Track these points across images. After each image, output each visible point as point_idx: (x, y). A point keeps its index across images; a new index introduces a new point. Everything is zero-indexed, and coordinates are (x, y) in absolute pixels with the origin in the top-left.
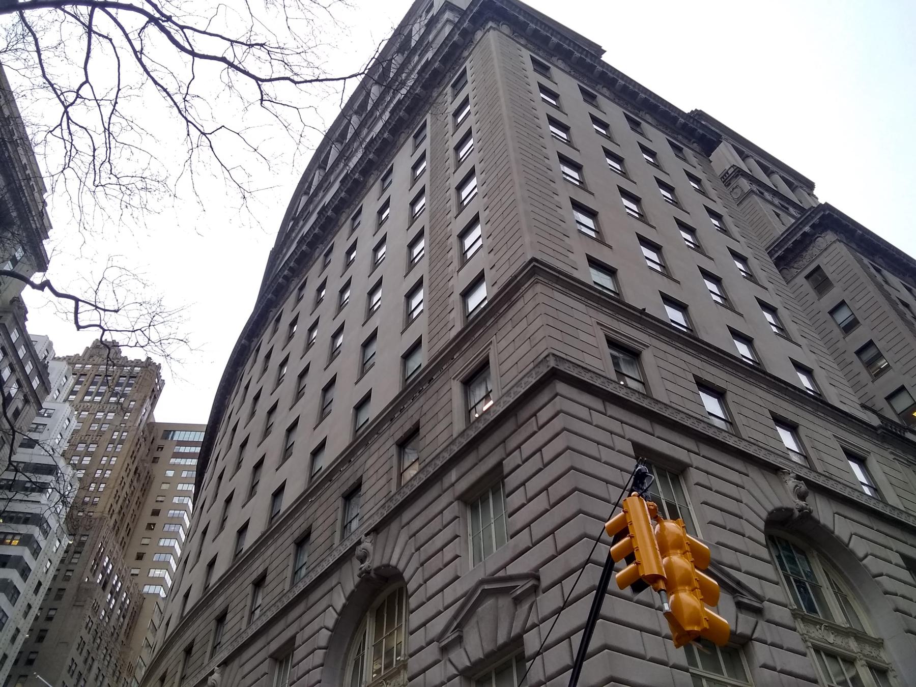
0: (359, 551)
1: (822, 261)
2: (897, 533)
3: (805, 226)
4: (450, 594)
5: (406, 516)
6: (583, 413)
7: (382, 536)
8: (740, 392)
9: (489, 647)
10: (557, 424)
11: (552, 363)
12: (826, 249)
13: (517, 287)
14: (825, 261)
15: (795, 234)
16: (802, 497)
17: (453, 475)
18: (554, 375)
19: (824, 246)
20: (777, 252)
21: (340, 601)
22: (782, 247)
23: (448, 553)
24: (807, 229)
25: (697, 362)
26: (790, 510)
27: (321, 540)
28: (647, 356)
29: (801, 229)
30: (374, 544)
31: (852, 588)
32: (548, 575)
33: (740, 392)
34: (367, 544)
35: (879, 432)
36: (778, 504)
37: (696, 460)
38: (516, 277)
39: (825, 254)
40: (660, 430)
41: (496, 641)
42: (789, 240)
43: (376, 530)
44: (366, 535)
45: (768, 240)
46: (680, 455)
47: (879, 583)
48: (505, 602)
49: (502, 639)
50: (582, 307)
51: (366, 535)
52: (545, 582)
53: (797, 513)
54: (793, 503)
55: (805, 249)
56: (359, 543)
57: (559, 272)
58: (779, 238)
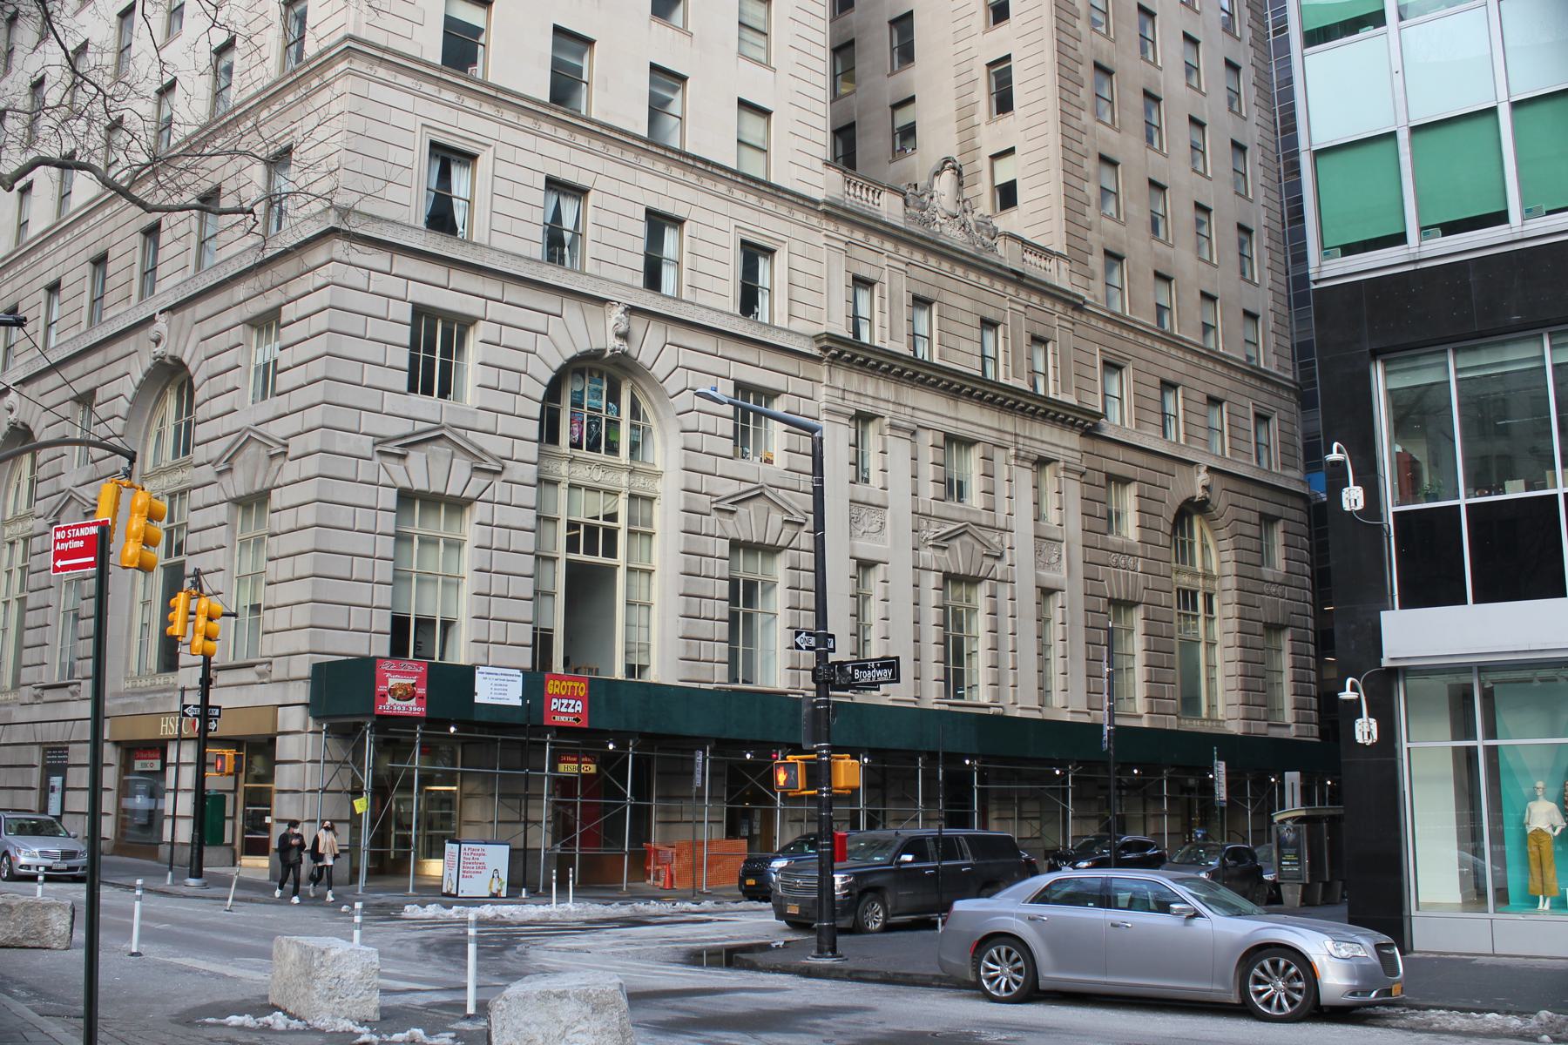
0: (152, 331)
2: (750, 354)
4: (227, 424)
5: (201, 309)
6: (356, 277)
7: (176, 317)
8: (612, 186)
9: (249, 490)
10: (324, 298)
11: (332, 221)
13: (329, 63)
16: (624, 336)
17: (241, 291)
18: (332, 233)
21: (138, 376)
23: (230, 379)
25: (562, 152)
26: (604, 351)
27: (119, 280)
28: (484, 162)
30: (169, 326)
31: (658, 420)
32: (295, 447)
33: (612, 186)
34: (161, 324)
36: (584, 346)
37: (495, 310)
38: (330, 49)
40: (459, 279)
41: (253, 484)
43: (172, 309)
44: (161, 312)
46: (471, 307)
47: (681, 422)
48: (263, 451)
49: (257, 487)
50: (405, 101)
51: (161, 312)
52: (290, 455)
53: (608, 354)
54: (613, 343)
56: (151, 320)
57: (385, 50)
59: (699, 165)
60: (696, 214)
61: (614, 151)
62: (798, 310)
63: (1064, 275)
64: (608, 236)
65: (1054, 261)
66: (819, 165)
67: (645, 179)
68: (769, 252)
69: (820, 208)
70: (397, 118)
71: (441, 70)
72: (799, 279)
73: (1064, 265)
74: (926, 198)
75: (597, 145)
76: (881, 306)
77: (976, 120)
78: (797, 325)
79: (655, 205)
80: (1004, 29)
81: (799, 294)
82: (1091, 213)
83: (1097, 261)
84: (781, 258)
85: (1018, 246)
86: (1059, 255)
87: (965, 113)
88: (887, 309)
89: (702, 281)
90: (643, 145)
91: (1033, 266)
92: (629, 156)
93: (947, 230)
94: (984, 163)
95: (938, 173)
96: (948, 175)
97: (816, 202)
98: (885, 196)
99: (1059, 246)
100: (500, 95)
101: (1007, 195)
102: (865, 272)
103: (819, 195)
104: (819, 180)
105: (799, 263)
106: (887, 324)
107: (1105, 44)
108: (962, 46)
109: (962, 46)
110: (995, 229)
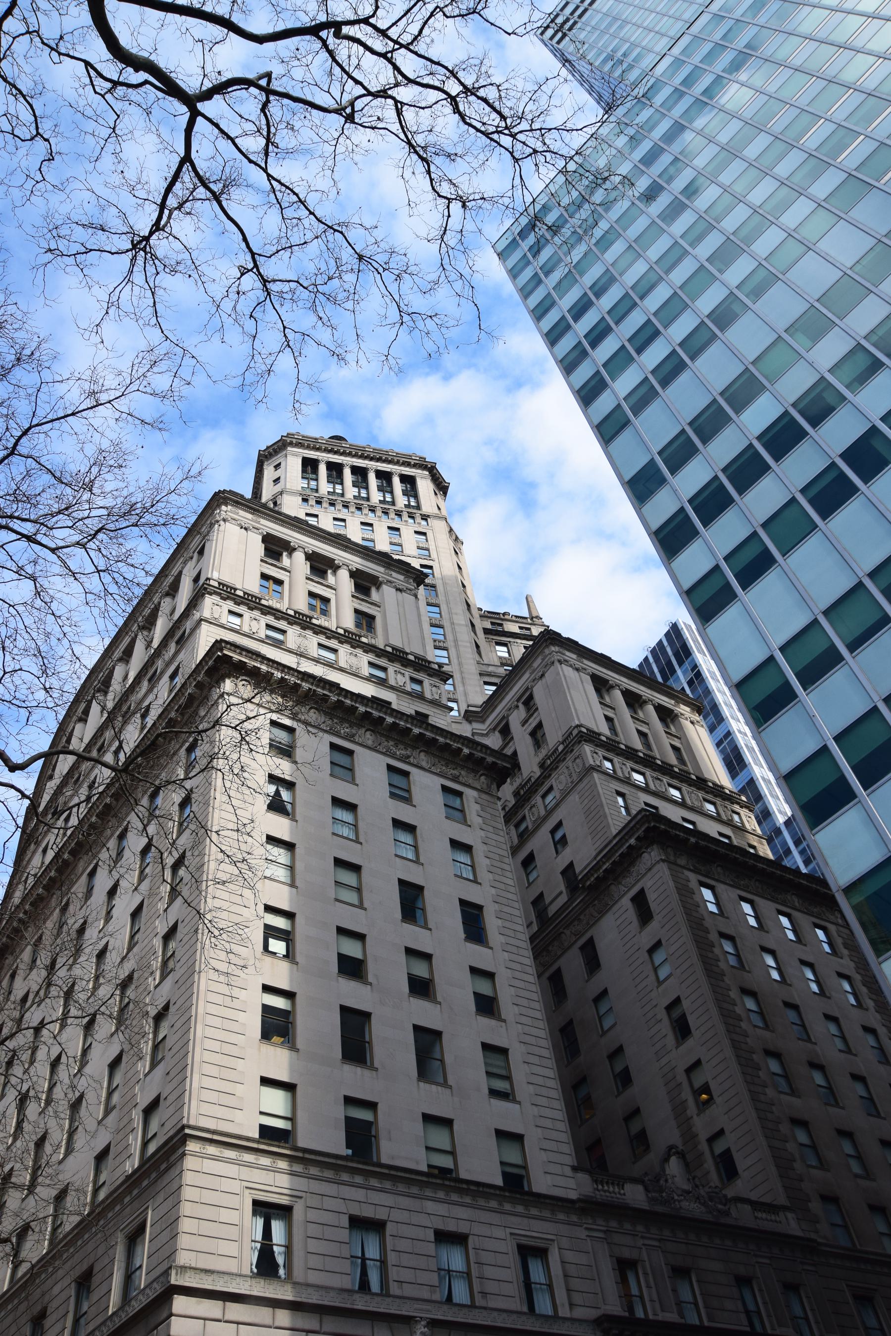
1: (647, 883)
3: (630, 838)
8: (403, 1216)
12: (650, 869)
14: (649, 884)
15: (622, 846)
19: (649, 864)
20: (604, 863)
22: (610, 858)
24: (632, 841)
29: (627, 841)
35: (577, 1206)
39: (649, 875)
42: (616, 851)
45: (602, 839)
50: (231, 1170)
55: (632, 863)
57: (214, 1132)
58: (611, 841)
59: (472, 1187)
60: (477, 1229)
61: (401, 1187)
62: (577, 1298)
63: (793, 1224)
64: (406, 1260)
65: (781, 1214)
66: (568, 1171)
67: (430, 1206)
68: (541, 1253)
69: (577, 1206)
70: (227, 1185)
71: (258, 1142)
72: (572, 1270)
73: (790, 1215)
74: (662, 1182)
75: (388, 1185)
76: (647, 1282)
77: (689, 1112)
78: (579, 1313)
79: (441, 1227)
80: (690, 1042)
81: (575, 1283)
82: (798, 1165)
83: (816, 1206)
84: (554, 1257)
85: (747, 1208)
86: (784, 1208)
87: (679, 1110)
88: (652, 1284)
89: (491, 1287)
90: (424, 1179)
91: (765, 1222)
92: (415, 1190)
93: (685, 1204)
94: (704, 1147)
95: (666, 1160)
96: (673, 1160)
97: (572, 1202)
98: (628, 1187)
99: (782, 1200)
100: (307, 1156)
101: (728, 1166)
102: (626, 1253)
103: (573, 1195)
104: (571, 1183)
105: (570, 1256)
106: (655, 1297)
107: (767, 1034)
108: (664, 1061)
109: (664, 1061)
110: (725, 1196)
